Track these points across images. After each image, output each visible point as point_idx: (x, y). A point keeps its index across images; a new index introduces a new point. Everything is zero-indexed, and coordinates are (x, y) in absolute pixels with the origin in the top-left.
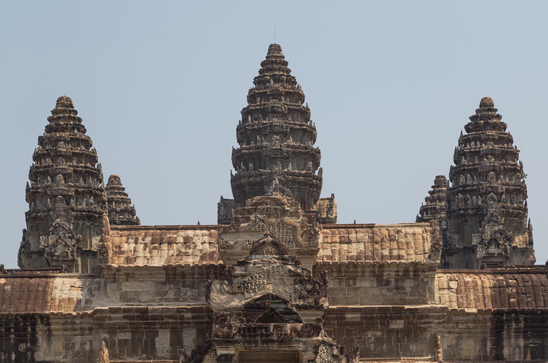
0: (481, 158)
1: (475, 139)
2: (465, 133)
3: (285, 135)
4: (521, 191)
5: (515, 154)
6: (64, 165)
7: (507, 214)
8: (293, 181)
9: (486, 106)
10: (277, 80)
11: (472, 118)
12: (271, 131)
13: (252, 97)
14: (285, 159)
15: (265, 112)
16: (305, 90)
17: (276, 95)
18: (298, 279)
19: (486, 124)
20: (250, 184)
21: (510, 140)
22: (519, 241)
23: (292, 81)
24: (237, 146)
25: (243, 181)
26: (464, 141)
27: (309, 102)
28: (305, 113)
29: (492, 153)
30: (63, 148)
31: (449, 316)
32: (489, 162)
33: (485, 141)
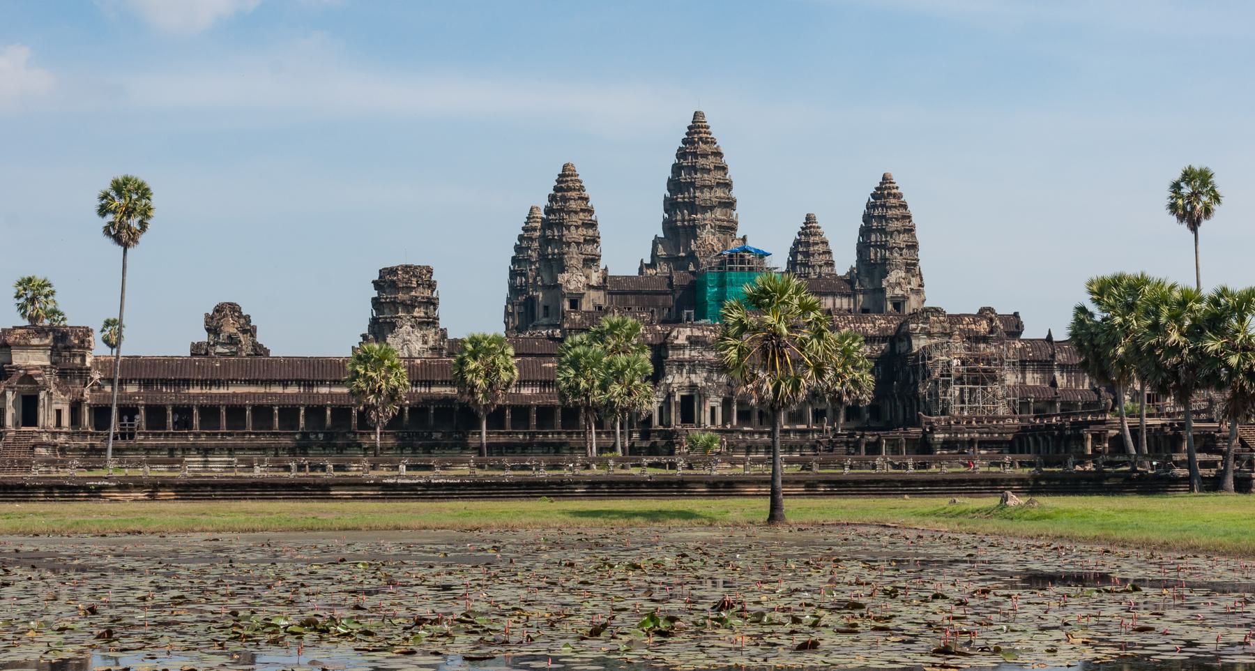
0: (887, 220)
1: (883, 206)
4: (913, 247)
6: (574, 218)
8: (720, 227)
10: (706, 143)
13: (681, 154)
15: (693, 169)
16: (722, 150)
17: (705, 156)
19: (889, 194)
20: (684, 226)
25: (679, 224)
30: (573, 205)
32: (894, 225)
33: (891, 207)
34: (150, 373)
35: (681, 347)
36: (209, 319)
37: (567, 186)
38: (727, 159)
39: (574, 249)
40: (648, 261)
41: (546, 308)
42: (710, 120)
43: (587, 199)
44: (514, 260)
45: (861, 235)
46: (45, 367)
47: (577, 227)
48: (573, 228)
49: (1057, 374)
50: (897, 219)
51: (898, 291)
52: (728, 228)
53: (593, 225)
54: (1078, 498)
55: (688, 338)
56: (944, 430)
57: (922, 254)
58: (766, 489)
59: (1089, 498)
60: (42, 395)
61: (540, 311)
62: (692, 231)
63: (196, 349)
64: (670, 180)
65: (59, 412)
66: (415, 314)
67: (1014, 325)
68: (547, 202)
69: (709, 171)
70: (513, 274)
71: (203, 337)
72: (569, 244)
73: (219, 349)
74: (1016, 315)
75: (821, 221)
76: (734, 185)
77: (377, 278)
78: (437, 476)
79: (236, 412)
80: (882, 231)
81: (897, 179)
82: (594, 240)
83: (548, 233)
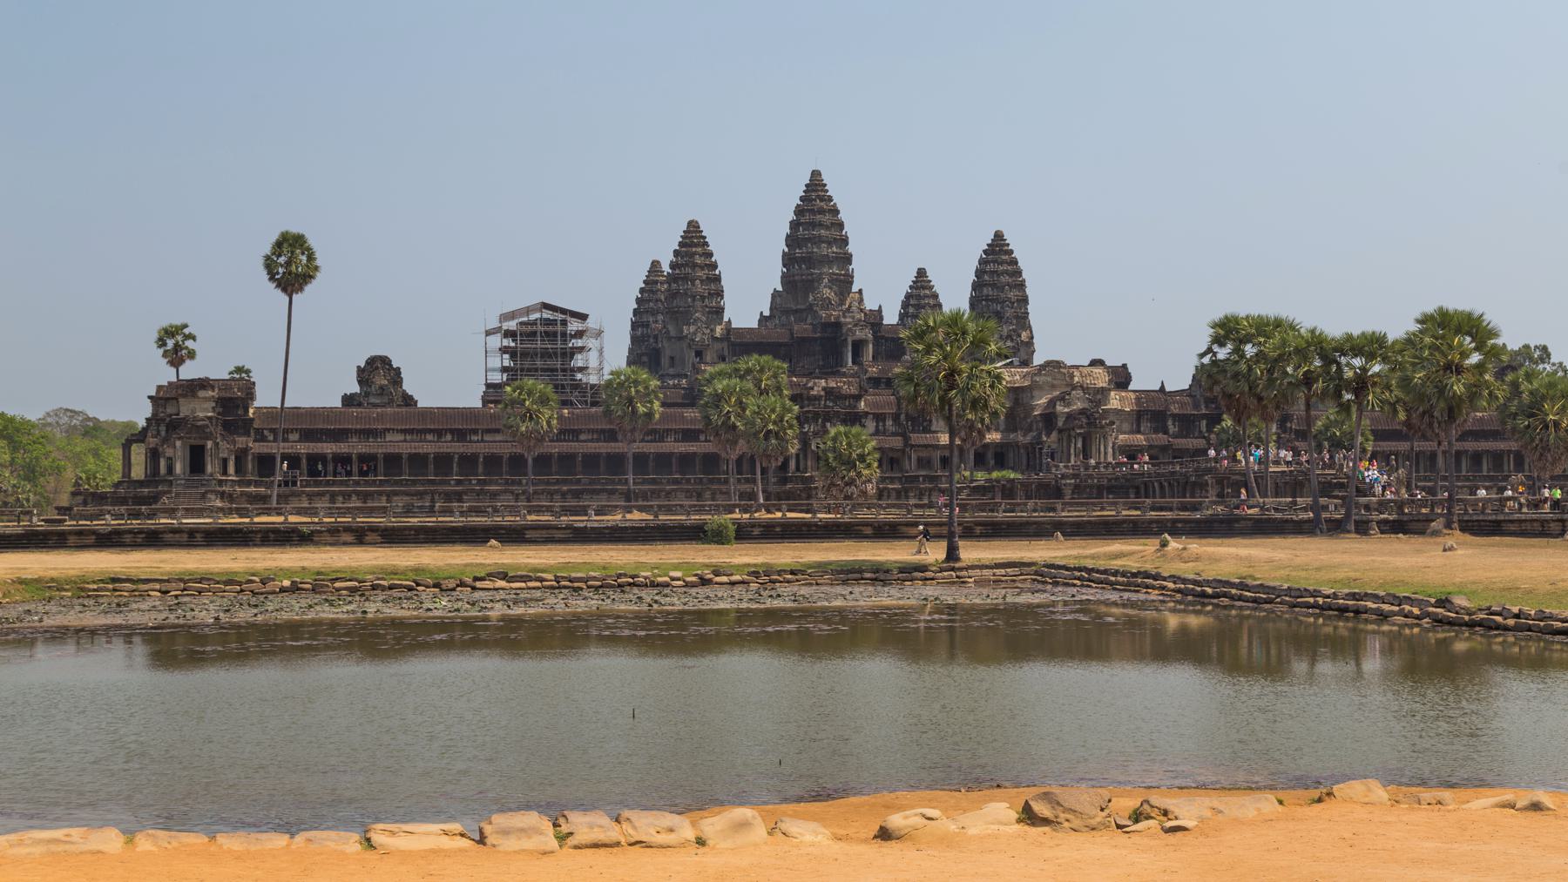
1: (994, 262)
3: (830, 244)
5: (1019, 273)
7: (1017, 317)
9: (999, 236)
12: (819, 240)
13: (799, 211)
15: (813, 225)
17: (822, 211)
18: (1091, 401)
21: (1016, 263)
22: (1024, 336)
23: (830, 199)
26: (982, 262)
28: (841, 225)
29: (1006, 272)
30: (698, 260)
31: (1117, 412)
32: (1005, 279)
33: (1001, 263)
34: (311, 424)
35: (817, 398)
36: (360, 371)
37: (693, 239)
38: (842, 216)
39: (698, 303)
40: (767, 313)
41: (672, 358)
42: (826, 178)
43: (711, 255)
44: (635, 312)
45: (974, 289)
46: (210, 418)
49: (1170, 423)
52: (844, 283)
53: (718, 279)
56: (1075, 476)
57: (1030, 308)
58: (945, 530)
60: (209, 444)
61: (665, 361)
62: (811, 284)
63: (348, 400)
64: (788, 236)
65: (225, 461)
67: (1121, 377)
68: (671, 257)
70: (634, 326)
71: (356, 389)
73: (373, 400)
74: (1124, 366)
75: (931, 275)
76: (850, 241)
78: (594, 520)
79: (393, 461)
80: (994, 286)
81: (1009, 238)
82: (720, 294)
83: (674, 286)
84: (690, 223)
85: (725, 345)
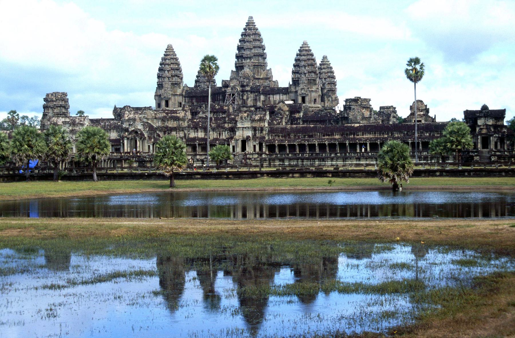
1: (300, 55)
2: (298, 52)
8: (255, 65)
11: (301, 47)
14: (250, 58)
17: (249, 35)
19: (303, 50)
20: (240, 66)
24: (237, 52)
27: (263, 36)
30: (167, 61)
47: (168, 71)
48: (166, 72)
50: (305, 61)
51: (303, 91)
52: (263, 66)
54: (75, 182)
55: (63, 122)
59: (78, 183)
66: (55, 111)
69: (251, 41)
72: (164, 78)
77: (45, 97)
84: (168, 46)
85: (181, 98)
